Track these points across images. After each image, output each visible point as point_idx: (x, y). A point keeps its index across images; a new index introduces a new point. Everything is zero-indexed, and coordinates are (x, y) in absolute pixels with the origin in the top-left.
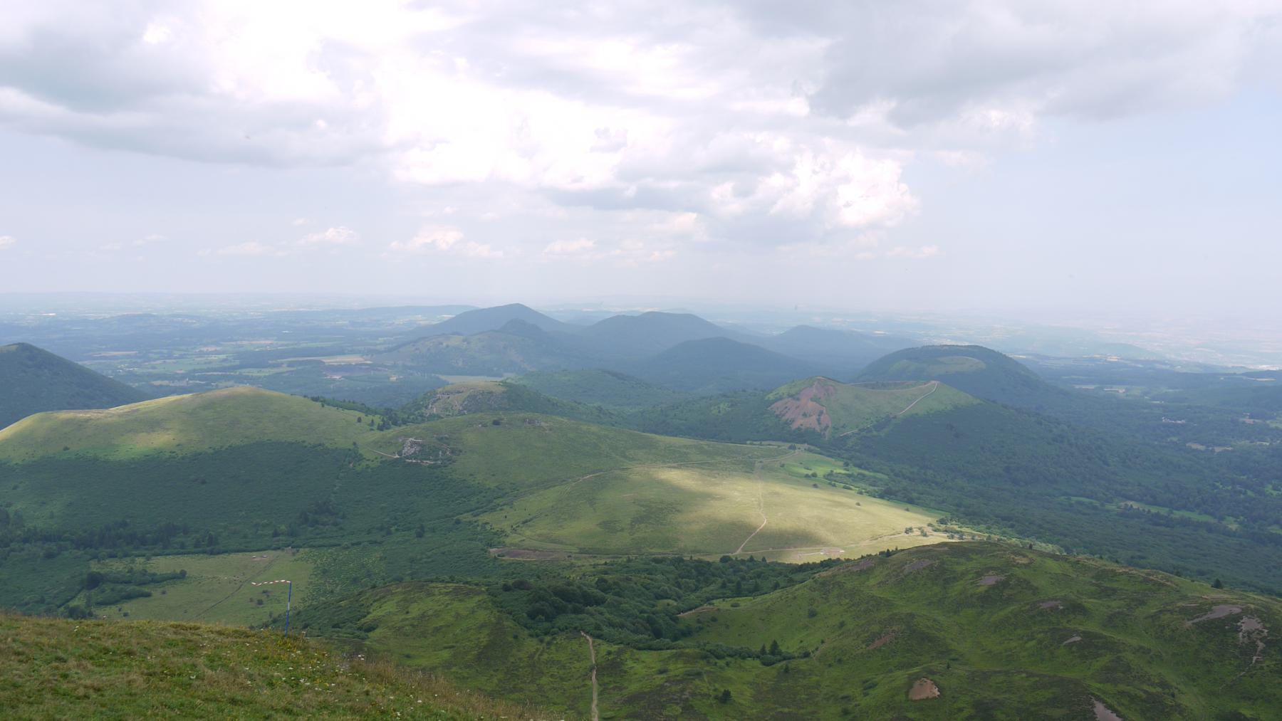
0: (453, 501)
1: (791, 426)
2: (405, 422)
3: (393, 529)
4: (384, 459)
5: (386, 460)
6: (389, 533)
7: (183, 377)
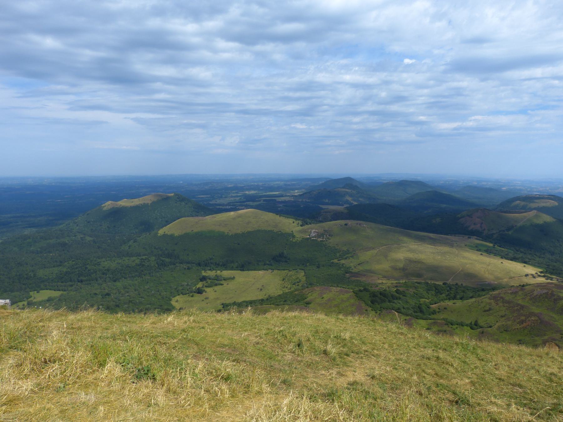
4: (303, 238)
7: (227, 205)
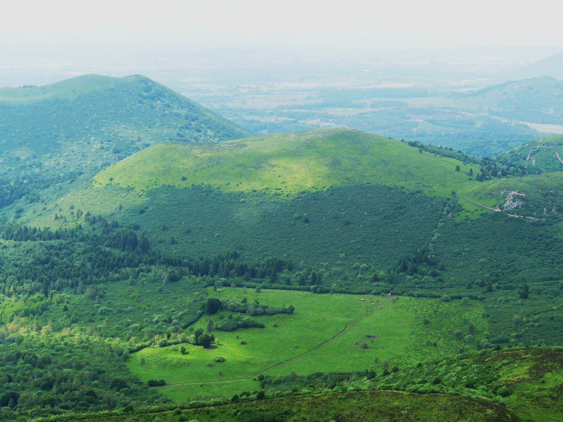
0: (558, 263)
2: (504, 174)
3: (494, 285)
4: (484, 212)
5: (486, 214)
6: (490, 290)
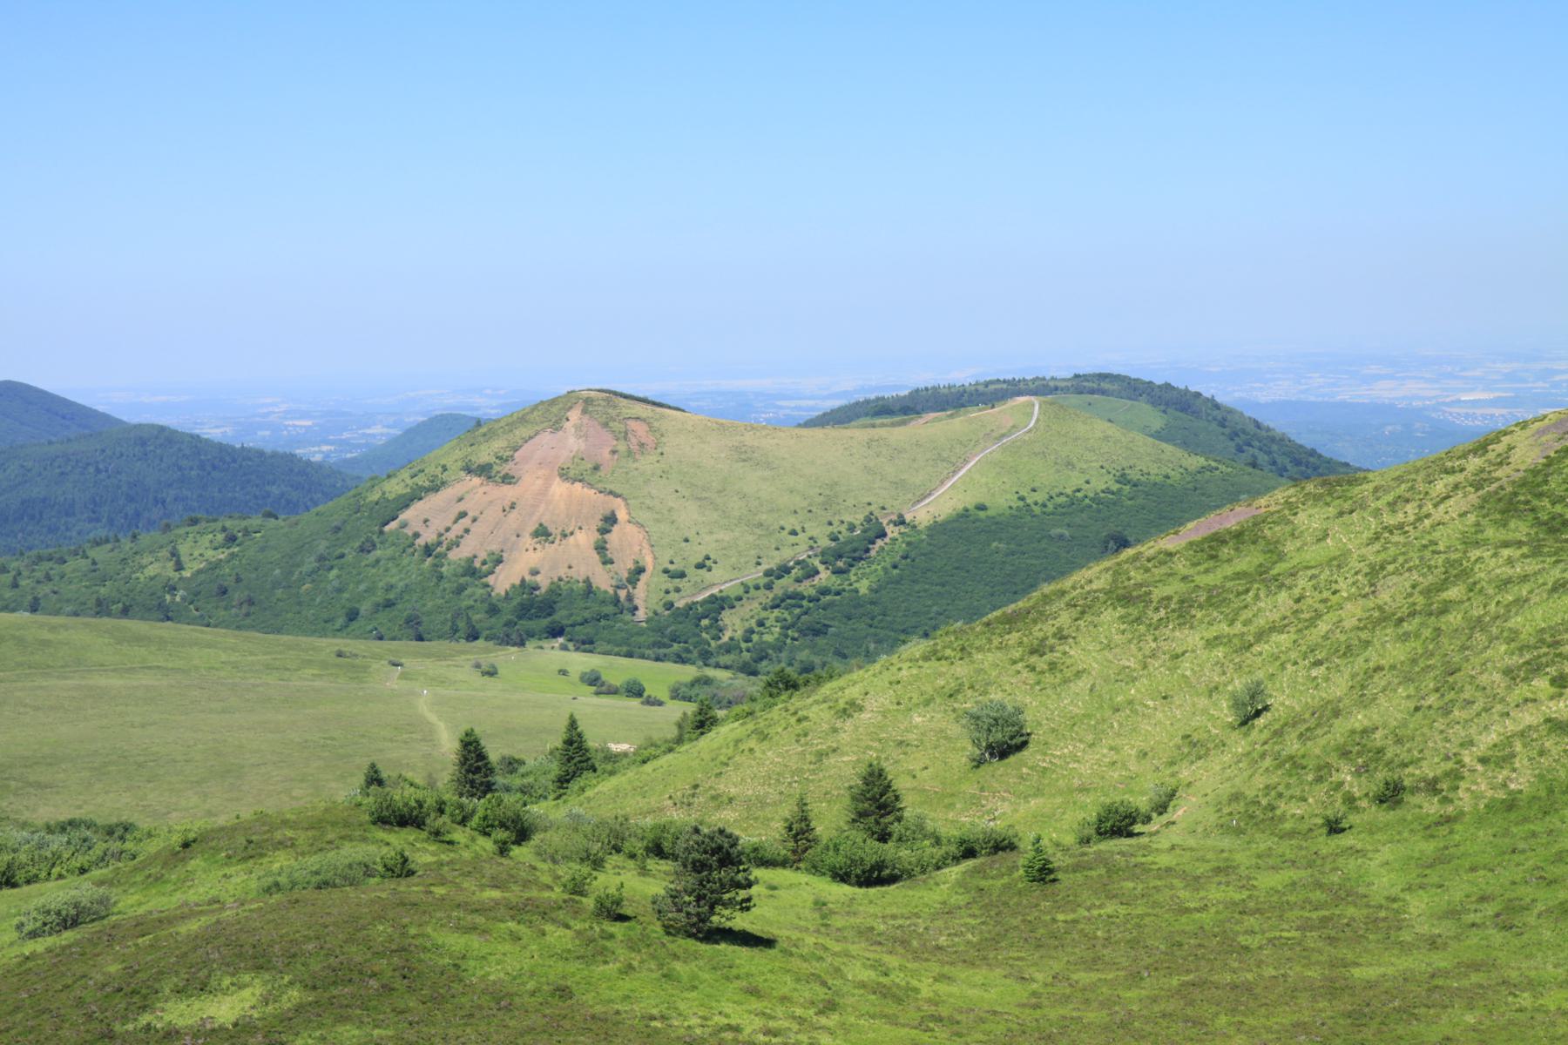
1: (490, 580)
